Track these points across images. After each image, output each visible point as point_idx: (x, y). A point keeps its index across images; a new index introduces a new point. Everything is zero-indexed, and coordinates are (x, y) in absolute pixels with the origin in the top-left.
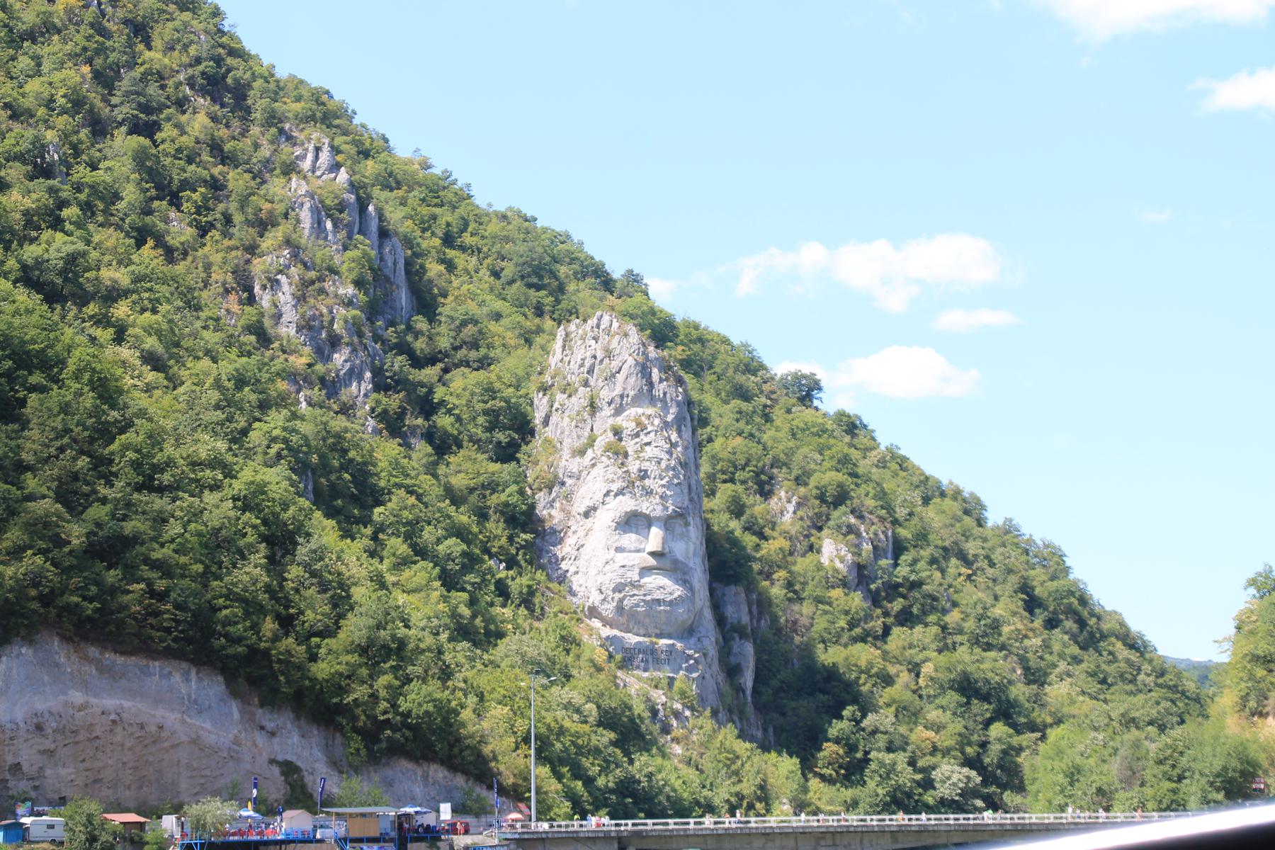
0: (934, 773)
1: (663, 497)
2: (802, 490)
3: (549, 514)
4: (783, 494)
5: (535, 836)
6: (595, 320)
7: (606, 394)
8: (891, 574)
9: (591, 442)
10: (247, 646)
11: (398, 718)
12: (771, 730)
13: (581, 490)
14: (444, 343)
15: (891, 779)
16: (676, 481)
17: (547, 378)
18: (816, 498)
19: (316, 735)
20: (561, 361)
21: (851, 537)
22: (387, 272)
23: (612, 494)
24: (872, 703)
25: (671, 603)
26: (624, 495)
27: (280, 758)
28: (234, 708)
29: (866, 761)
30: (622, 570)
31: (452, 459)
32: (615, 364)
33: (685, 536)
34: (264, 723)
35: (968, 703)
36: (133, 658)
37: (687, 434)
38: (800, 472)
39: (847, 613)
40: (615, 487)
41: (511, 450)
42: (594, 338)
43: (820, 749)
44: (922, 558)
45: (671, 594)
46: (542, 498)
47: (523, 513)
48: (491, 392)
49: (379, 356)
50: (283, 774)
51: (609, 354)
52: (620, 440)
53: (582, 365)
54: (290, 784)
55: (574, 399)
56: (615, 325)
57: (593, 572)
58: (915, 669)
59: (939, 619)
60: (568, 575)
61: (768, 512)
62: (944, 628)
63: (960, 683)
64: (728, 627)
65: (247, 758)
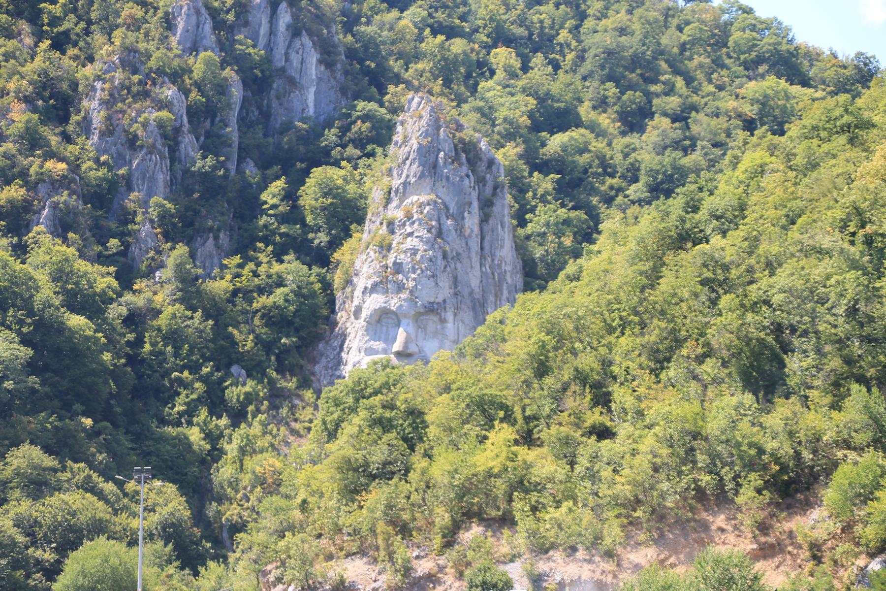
7: (396, 182)
22: (292, 72)
33: (440, 334)
37: (472, 222)
46: (339, 295)
48: (328, 191)
56: (422, 106)
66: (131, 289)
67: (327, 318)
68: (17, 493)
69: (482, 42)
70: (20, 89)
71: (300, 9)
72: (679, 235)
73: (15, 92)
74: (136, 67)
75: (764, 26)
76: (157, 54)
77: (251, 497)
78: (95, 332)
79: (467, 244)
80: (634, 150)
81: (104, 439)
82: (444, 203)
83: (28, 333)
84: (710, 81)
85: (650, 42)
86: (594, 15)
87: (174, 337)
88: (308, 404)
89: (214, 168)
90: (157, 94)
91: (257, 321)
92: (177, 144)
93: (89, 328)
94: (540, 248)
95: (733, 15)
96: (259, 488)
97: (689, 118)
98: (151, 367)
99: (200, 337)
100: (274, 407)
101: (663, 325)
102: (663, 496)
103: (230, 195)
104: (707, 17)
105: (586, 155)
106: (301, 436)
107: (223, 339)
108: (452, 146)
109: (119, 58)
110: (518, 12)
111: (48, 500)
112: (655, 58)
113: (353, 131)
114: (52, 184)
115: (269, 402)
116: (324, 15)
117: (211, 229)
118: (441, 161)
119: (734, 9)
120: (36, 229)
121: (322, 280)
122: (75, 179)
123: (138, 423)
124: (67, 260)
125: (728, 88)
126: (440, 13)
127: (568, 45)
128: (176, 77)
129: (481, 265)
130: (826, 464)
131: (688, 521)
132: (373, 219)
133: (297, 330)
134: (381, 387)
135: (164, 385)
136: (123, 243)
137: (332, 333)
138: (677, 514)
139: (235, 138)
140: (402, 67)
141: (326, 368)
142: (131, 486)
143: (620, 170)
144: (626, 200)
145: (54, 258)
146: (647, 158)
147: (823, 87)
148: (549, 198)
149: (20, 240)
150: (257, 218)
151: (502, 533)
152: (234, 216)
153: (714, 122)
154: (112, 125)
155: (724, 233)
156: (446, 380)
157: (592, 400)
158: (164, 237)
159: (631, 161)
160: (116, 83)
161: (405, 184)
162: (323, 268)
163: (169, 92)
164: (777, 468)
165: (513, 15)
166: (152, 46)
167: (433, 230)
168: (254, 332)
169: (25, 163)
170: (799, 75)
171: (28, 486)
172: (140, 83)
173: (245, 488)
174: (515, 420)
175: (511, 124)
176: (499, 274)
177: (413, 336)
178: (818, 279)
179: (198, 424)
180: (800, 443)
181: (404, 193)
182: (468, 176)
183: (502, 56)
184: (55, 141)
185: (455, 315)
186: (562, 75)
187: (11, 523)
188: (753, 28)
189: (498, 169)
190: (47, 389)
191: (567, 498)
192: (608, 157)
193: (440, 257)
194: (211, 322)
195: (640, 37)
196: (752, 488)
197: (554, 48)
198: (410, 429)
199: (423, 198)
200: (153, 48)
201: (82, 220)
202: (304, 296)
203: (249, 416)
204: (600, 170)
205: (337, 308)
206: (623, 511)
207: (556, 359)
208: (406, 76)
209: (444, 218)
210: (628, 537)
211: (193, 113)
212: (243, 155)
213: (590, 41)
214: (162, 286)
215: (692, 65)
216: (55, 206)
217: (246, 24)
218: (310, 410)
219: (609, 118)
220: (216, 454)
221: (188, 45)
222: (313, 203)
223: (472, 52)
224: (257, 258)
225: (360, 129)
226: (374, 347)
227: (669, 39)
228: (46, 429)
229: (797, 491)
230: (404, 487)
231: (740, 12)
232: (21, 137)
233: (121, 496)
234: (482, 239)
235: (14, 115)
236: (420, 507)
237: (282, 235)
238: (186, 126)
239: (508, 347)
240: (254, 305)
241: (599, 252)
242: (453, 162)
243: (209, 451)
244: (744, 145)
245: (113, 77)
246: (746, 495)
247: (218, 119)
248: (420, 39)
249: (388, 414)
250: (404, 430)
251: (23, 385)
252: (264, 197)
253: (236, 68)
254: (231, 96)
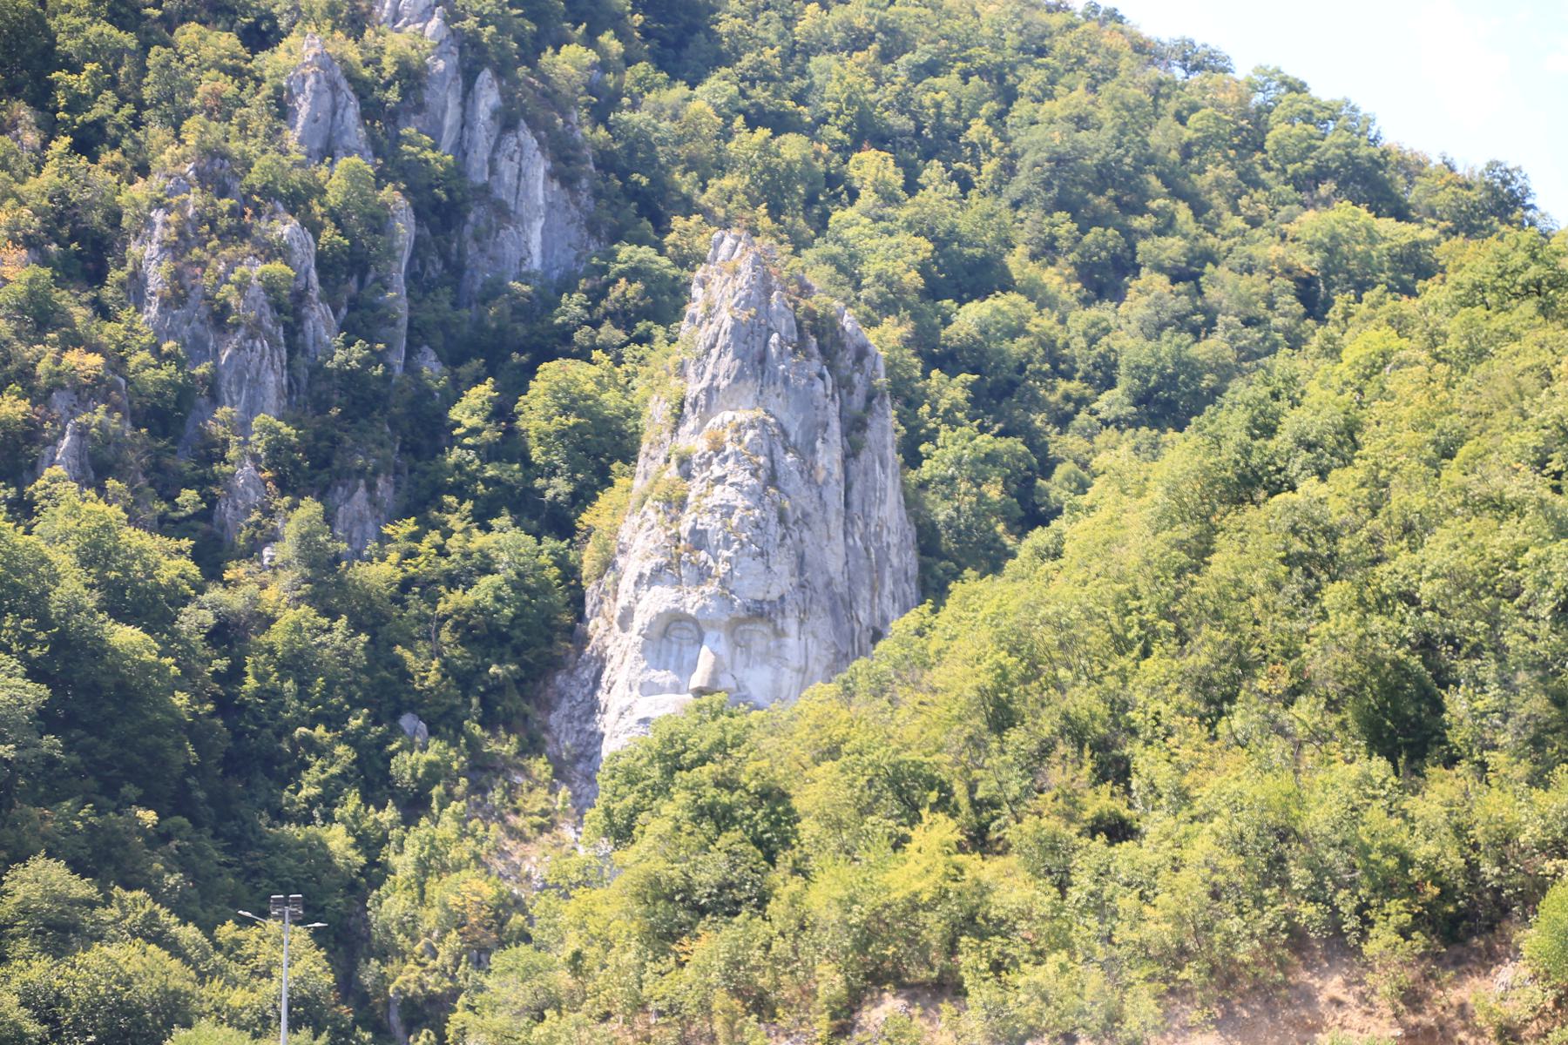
7: (694, 388)
22: (502, 194)
30: (641, 729)
32: (714, 328)
33: (774, 657)
37: (829, 457)
46: (591, 589)
48: (570, 403)
66: (221, 579)
67: (571, 630)
68: (24, 946)
69: (834, 141)
70: (17, 224)
71: (516, 82)
72: (1242, 477)
73: (8, 229)
74: (225, 184)
75: (1326, 114)
76: (265, 161)
77: (440, 950)
78: (161, 654)
79: (820, 497)
80: (1107, 331)
81: (178, 848)
82: (780, 425)
83: (40, 658)
84: (1236, 211)
85: (1130, 141)
86: (1031, 94)
87: (297, 664)
88: (538, 783)
89: (366, 363)
90: (264, 232)
91: (445, 636)
92: (300, 320)
93: (149, 649)
94: (946, 504)
95: (1272, 94)
96: (455, 932)
97: (1202, 274)
98: (256, 718)
99: (345, 664)
100: (479, 788)
101: (1221, 636)
102: (1229, 942)
103: (395, 410)
104: (1228, 98)
105: (1022, 341)
106: (526, 840)
107: (386, 668)
108: (793, 323)
109: (195, 168)
110: (897, 88)
111: (81, 958)
112: (1139, 170)
113: (612, 297)
114: (77, 393)
115: (470, 780)
116: (556, 92)
117: (361, 472)
118: (773, 350)
119: (1273, 85)
120: (49, 472)
121: (561, 561)
122: (118, 383)
123: (235, 818)
124: (106, 528)
125: (1268, 222)
126: (759, 89)
127: (987, 147)
128: (297, 201)
129: (846, 534)
130: (1522, 885)
131: (1276, 986)
132: (652, 453)
133: (517, 652)
134: (711, 750)
135: (281, 750)
136: (204, 497)
137: (579, 656)
138: (1256, 975)
139: (402, 310)
140: (695, 184)
141: (570, 718)
142: (227, 931)
143: (1081, 366)
144: (1093, 419)
145: (84, 525)
146: (1130, 346)
147: (1432, 221)
148: (959, 415)
149: (21, 492)
150: (443, 452)
151: (938, 1011)
152: (402, 449)
153: (1245, 281)
154: (182, 287)
155: (1322, 474)
156: (830, 737)
157: (1094, 770)
158: (278, 485)
159: (1102, 350)
160: (190, 212)
161: (710, 391)
162: (562, 540)
163: (285, 228)
164: (1437, 891)
165: (888, 93)
166: (252, 147)
167: (760, 472)
168: (440, 654)
169: (27, 355)
170: (1389, 201)
171: (43, 933)
172: (233, 212)
173: (429, 934)
174: (956, 807)
175: (889, 285)
176: (877, 551)
177: (726, 660)
178: (1499, 554)
179: (343, 820)
180: (1475, 847)
181: (708, 406)
182: (822, 376)
183: (871, 166)
184: (80, 315)
185: (801, 622)
186: (975, 199)
187: (16, 999)
188: (1308, 117)
189: (875, 364)
190: (75, 758)
191: (1054, 948)
192: (1059, 343)
193: (774, 520)
194: (364, 638)
195: (1111, 133)
196: (1391, 927)
197: (961, 151)
198: (766, 825)
199: (743, 416)
200: (254, 151)
201: (131, 456)
202: (528, 590)
203: (434, 804)
204: (1047, 366)
205: (588, 611)
206: (1159, 970)
207: (1023, 699)
208: (703, 200)
209: (779, 450)
210: (1168, 1015)
211: (327, 265)
212: (418, 339)
213: (1021, 140)
214: (275, 574)
215: (1203, 181)
216: (82, 432)
217: (420, 107)
218: (541, 793)
219: (1061, 274)
220: (376, 873)
221: (317, 145)
222: (544, 424)
223: (816, 159)
224: (445, 523)
225: (624, 293)
226: (657, 680)
227: (1163, 137)
228: (74, 830)
229: (1471, 932)
230: (762, 929)
231: (1283, 90)
232: (20, 309)
233: (211, 949)
234: (848, 489)
235: (9, 271)
236: (787, 965)
237: (487, 482)
238: (316, 289)
239: (938, 676)
240: (440, 607)
241: (1092, 508)
242: (795, 352)
243: (363, 868)
244: (1345, 319)
245: (185, 202)
246: (1382, 939)
247: (371, 277)
248: (726, 134)
249: (725, 798)
250: (755, 826)
251: (32, 751)
252: (455, 413)
253: (403, 186)
254: (394, 235)
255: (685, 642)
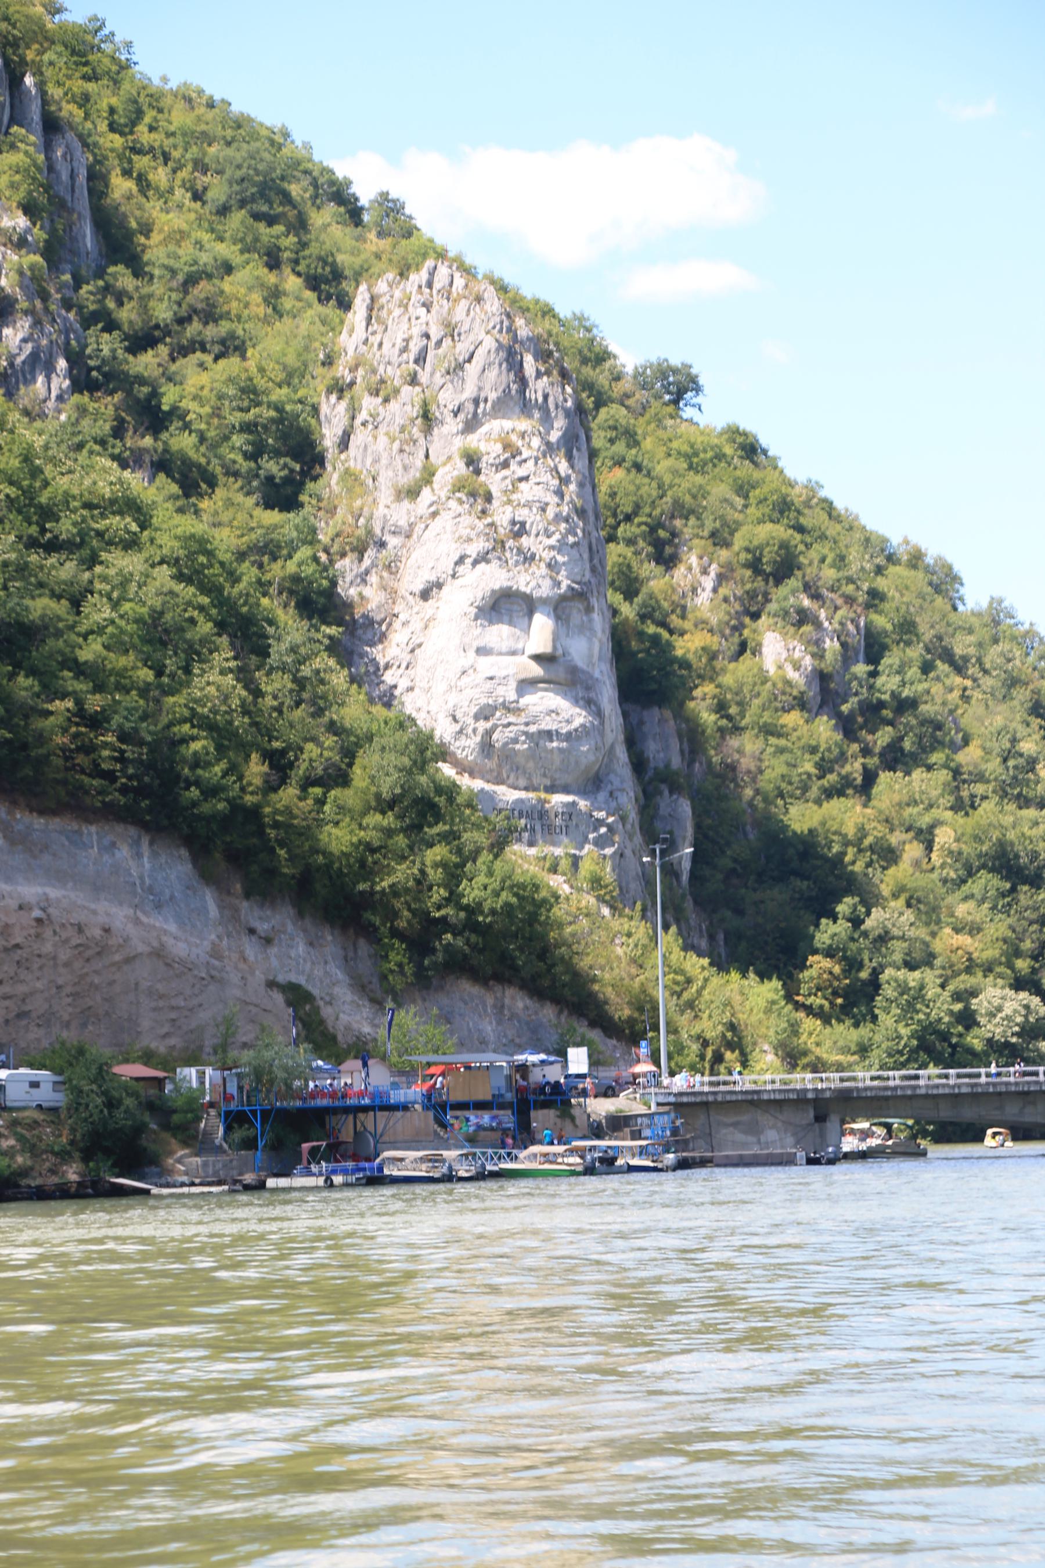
0: (974, 1001)
1: (552, 566)
2: (724, 554)
3: (360, 594)
4: (694, 560)
5: (698, 1099)
6: (424, 275)
8: (871, 687)
9: (428, 476)
10: (227, 800)
11: (462, 915)
12: (721, 937)
13: (413, 556)
14: (163, 313)
15: (917, 1012)
16: (571, 539)
17: (341, 371)
18: (747, 565)
19: (330, 941)
20: (366, 342)
21: (807, 629)
23: (469, 561)
24: (870, 892)
25: (568, 737)
26: (488, 562)
27: (281, 979)
28: (209, 899)
29: (874, 985)
30: (489, 685)
31: (205, 504)
32: (463, 348)
33: (585, 629)
34: (256, 924)
35: (1013, 890)
36: (57, 820)
38: (718, 524)
39: (813, 750)
40: (473, 550)
41: (289, 490)
42: (424, 305)
43: (803, 966)
44: (911, 661)
45: (568, 722)
46: (346, 565)
47: (322, 593)
48: (250, 393)
49: (75, 332)
50: (289, 1003)
51: (451, 331)
52: (478, 472)
53: (405, 350)
54: (301, 1020)
55: (394, 406)
57: (442, 687)
58: (926, 837)
59: (948, 757)
60: (397, 693)
61: (674, 590)
62: (956, 772)
63: (994, 858)
64: (650, 773)
65: (234, 978)
255: (515, 614)
